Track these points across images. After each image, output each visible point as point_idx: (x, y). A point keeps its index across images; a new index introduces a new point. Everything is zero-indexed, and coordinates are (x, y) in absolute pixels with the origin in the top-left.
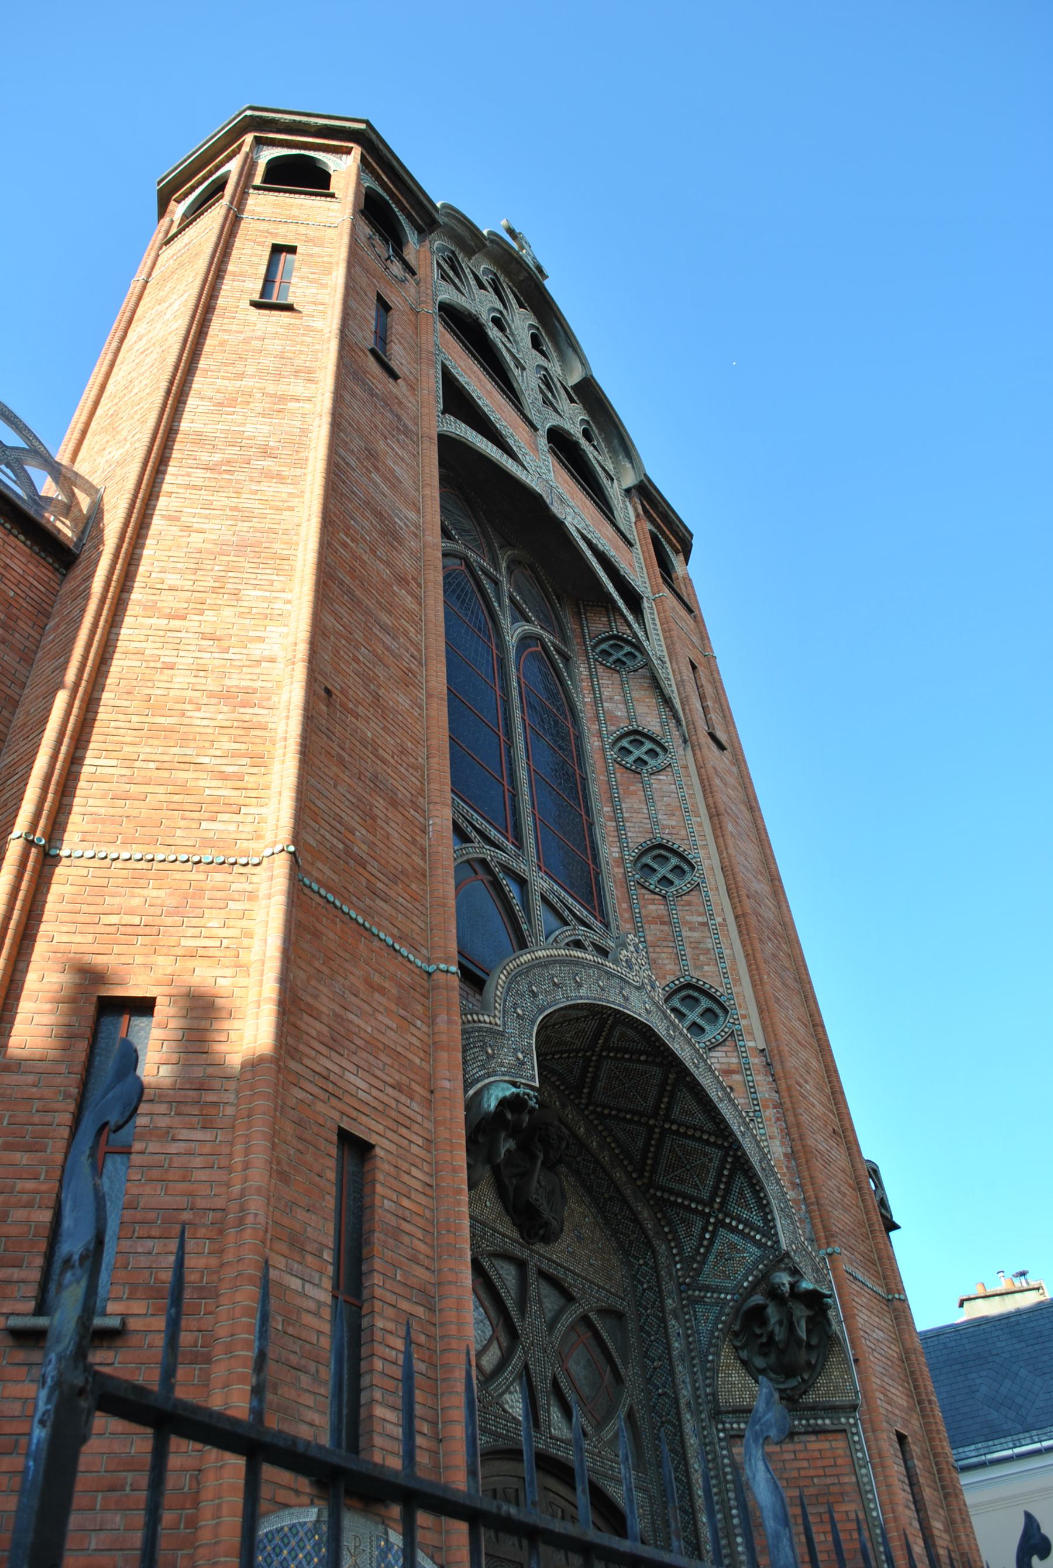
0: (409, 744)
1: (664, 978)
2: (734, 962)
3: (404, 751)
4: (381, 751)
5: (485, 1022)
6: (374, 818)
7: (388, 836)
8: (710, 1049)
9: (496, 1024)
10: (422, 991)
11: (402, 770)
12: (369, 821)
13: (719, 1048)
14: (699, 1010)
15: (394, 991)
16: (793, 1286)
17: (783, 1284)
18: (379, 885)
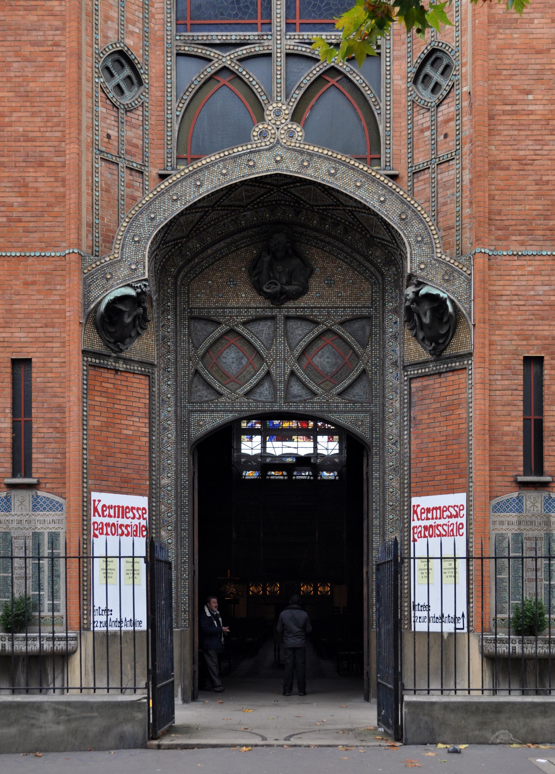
0: (53, 109)
1: (420, 49)
2: (466, 13)
3: (49, 117)
4: (31, 135)
5: (106, 261)
6: (26, 186)
7: (37, 190)
8: (438, 106)
9: (115, 258)
10: (61, 268)
11: (47, 134)
12: (22, 190)
13: (445, 102)
14: (432, 73)
15: (42, 279)
16: (416, 293)
17: (408, 295)
18: (32, 224)
